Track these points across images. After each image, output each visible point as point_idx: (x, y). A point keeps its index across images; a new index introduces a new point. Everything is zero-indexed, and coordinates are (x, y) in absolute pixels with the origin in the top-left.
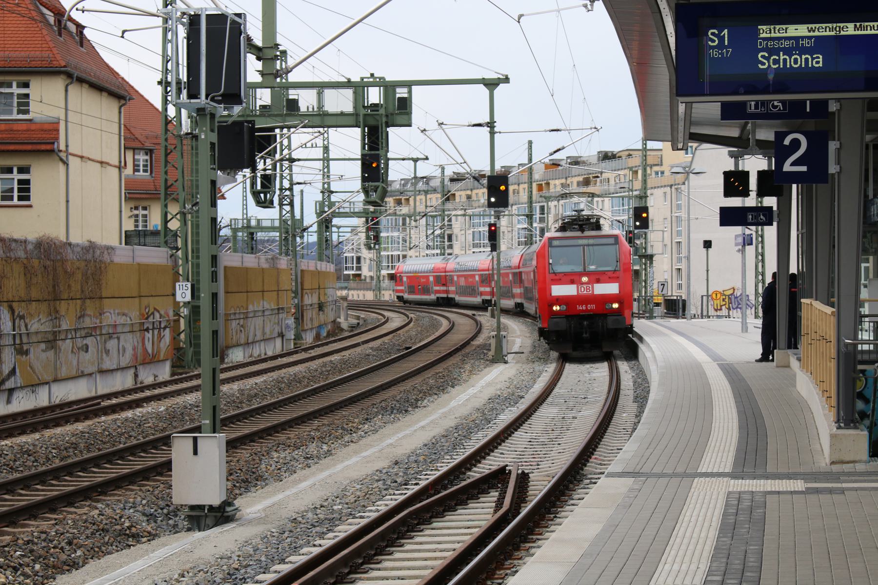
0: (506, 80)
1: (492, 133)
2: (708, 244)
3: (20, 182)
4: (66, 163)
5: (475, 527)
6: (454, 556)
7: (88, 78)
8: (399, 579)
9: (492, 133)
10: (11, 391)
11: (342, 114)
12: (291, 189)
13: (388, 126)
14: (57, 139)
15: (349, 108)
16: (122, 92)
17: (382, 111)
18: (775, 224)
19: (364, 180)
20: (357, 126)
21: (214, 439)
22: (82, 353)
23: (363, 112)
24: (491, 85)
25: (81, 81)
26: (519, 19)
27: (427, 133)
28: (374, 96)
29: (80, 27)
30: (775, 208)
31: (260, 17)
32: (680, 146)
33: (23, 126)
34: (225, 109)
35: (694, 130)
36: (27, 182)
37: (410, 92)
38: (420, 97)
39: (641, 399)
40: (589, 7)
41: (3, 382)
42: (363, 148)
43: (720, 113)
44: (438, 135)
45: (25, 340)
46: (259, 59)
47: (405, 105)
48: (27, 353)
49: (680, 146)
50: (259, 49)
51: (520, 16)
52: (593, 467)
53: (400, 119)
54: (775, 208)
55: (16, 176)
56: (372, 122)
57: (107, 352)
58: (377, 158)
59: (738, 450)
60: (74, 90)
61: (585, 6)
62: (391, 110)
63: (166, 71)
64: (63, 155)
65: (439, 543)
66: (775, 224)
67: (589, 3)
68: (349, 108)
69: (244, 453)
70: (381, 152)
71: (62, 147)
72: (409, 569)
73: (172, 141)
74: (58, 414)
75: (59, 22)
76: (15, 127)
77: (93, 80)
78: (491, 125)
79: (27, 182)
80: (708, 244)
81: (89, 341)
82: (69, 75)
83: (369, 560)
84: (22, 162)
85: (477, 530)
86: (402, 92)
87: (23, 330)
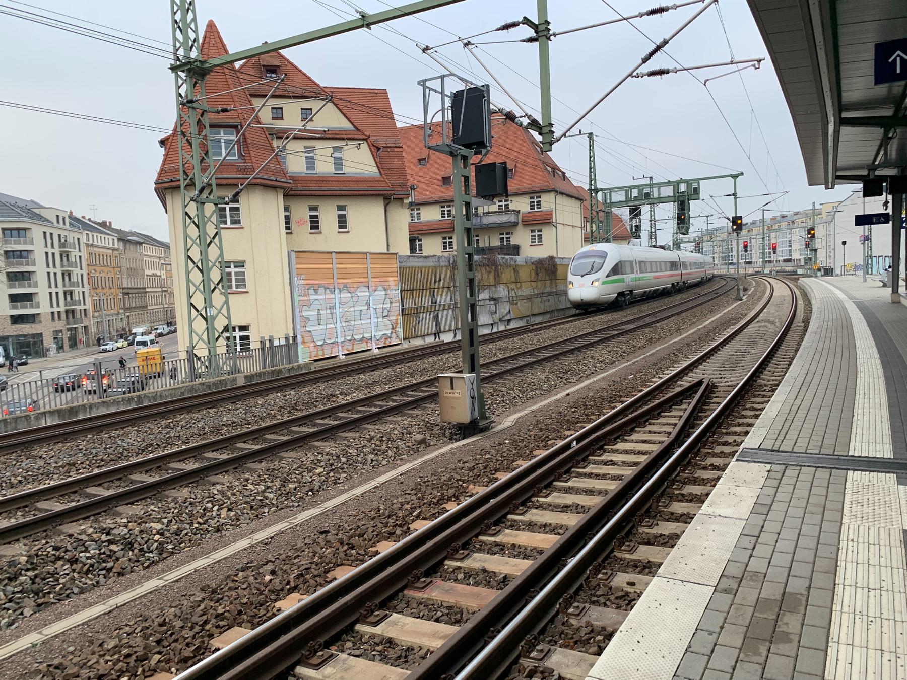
0: (742, 174)
1: (736, 198)
2: (844, 243)
3: (538, 235)
4: (556, 227)
5: (644, 453)
6: (561, 542)
7: (565, 192)
8: (599, 475)
9: (736, 198)
10: (509, 321)
11: (669, 197)
12: (655, 232)
13: (689, 200)
14: (552, 217)
15: (672, 194)
16: (581, 198)
17: (686, 194)
18: (891, 222)
19: (678, 224)
20: (674, 202)
21: (462, 379)
22: (546, 303)
23: (677, 195)
24: (735, 177)
25: (562, 194)
26: (706, 81)
27: (428, 51)
28: (683, 188)
29: (564, 173)
30: (891, 214)
31: (540, 110)
32: (830, 186)
33: (539, 214)
34: (476, 153)
35: (838, 174)
36: (541, 235)
37: (699, 185)
38: (704, 187)
39: (806, 322)
40: (757, 66)
41: (504, 317)
42: (678, 210)
43: (873, 70)
44: (711, 202)
45: (515, 299)
46: (540, 134)
47: (697, 191)
48: (516, 304)
49: (830, 186)
50: (541, 128)
51: (706, 81)
52: (766, 375)
53: (696, 197)
54: (891, 214)
55: (536, 234)
56: (681, 199)
57: (560, 302)
58: (684, 214)
59: (890, 406)
60: (559, 198)
61: (754, 66)
62: (690, 193)
63: (591, 185)
64: (554, 224)
65: (645, 442)
66: (891, 222)
67: (756, 63)
68: (672, 194)
69: (488, 388)
70: (686, 212)
71: (554, 220)
72: (628, 454)
73: (593, 212)
74: (438, 349)
75: (553, 172)
76: (536, 214)
77: (568, 193)
78: (735, 195)
79: (541, 235)
80: (844, 243)
81: (549, 297)
82: (556, 192)
83: (514, 510)
84: (539, 227)
85: (645, 457)
86: (695, 185)
87: (514, 295)
